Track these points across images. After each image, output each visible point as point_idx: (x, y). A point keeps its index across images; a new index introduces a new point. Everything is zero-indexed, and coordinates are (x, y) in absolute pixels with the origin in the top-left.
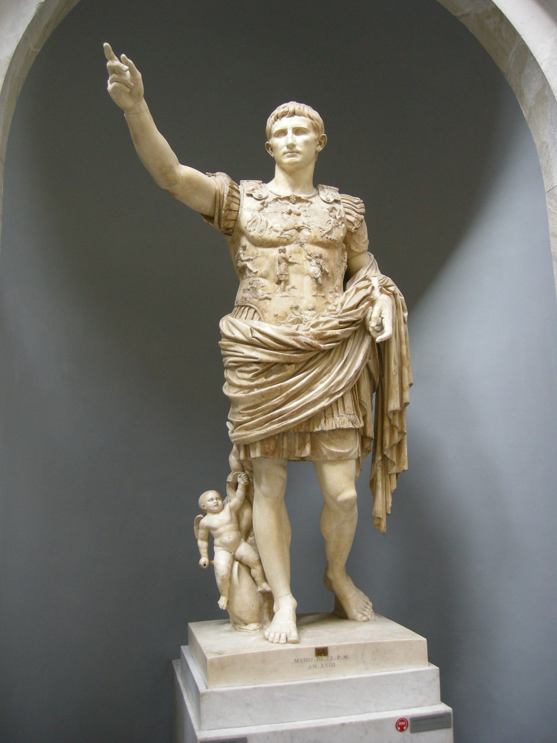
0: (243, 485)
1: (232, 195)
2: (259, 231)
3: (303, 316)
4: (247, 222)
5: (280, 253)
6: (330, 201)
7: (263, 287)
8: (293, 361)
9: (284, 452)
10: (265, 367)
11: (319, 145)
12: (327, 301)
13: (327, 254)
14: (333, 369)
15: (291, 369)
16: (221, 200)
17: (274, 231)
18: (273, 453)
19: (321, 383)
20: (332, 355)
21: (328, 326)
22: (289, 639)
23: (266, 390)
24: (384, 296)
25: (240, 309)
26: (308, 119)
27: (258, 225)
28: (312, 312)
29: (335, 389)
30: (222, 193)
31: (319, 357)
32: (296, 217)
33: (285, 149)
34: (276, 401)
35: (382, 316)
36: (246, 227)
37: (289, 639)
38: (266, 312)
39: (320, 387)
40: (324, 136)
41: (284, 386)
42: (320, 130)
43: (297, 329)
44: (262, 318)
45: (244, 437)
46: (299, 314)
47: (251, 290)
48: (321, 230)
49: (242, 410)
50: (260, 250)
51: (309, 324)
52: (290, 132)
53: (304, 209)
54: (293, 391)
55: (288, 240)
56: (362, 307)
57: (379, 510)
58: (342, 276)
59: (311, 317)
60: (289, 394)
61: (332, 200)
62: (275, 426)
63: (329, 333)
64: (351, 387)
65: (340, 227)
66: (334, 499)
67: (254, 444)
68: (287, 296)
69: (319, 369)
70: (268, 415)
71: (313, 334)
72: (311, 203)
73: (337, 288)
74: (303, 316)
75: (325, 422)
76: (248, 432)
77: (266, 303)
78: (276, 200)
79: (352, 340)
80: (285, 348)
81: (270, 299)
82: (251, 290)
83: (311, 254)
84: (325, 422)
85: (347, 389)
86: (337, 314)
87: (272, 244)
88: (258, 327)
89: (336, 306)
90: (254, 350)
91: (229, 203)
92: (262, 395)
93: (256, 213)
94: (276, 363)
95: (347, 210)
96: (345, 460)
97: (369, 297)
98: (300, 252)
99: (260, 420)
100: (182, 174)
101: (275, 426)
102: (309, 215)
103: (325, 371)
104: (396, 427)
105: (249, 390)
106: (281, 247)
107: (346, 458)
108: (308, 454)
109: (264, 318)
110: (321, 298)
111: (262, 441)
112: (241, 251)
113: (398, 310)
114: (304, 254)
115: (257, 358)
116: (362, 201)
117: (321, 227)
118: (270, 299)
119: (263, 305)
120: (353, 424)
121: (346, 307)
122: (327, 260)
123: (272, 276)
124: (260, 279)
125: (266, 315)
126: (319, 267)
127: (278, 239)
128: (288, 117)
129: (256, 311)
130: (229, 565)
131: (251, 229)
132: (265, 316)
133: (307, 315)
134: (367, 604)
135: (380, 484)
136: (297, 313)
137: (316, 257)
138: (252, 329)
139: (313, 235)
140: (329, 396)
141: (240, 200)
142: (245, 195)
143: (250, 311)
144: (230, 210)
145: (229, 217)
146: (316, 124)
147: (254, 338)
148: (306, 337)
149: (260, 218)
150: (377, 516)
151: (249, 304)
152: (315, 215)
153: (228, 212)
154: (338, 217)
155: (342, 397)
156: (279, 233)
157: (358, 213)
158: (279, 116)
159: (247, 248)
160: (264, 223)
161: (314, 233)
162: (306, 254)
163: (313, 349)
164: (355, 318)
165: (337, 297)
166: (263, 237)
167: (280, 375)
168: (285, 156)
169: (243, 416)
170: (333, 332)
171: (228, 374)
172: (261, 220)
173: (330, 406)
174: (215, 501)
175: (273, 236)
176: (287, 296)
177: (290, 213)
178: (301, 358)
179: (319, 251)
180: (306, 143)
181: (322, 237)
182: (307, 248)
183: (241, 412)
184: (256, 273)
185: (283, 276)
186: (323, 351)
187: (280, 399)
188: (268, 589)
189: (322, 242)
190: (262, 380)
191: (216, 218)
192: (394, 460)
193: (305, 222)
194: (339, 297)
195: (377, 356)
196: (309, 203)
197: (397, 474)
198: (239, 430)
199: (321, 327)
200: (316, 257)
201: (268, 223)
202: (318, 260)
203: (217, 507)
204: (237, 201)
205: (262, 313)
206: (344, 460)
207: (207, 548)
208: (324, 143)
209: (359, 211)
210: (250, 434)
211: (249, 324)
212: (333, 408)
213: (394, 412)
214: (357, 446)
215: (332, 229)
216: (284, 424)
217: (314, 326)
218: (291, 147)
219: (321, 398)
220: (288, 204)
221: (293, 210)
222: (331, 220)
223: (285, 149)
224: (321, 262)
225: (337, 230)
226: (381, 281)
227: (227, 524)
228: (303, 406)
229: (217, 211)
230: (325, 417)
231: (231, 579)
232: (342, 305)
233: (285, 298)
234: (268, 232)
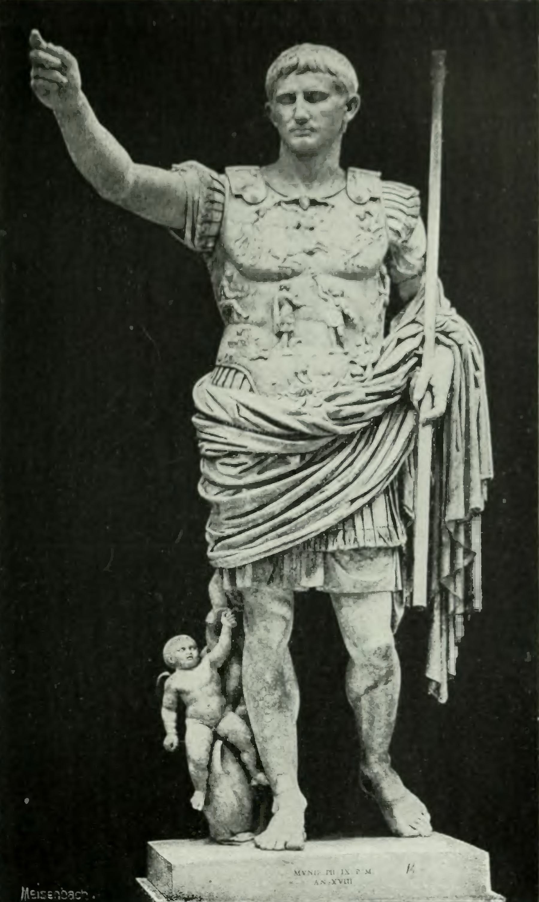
0: (229, 627)
4: (234, 241)
10: (257, 460)
17: (272, 256)
20: (355, 440)
22: (288, 845)
25: (223, 371)
26: (328, 76)
30: (196, 198)
33: (292, 124)
35: (432, 383)
37: (288, 845)
44: (254, 388)
47: (240, 344)
52: (300, 98)
55: (293, 270)
61: (366, 198)
67: (242, 568)
78: (279, 204)
79: (386, 418)
84: (344, 538)
86: (365, 380)
89: (365, 368)
104: (460, 544)
105: (235, 490)
106: (284, 282)
116: (416, 192)
120: (385, 541)
121: (379, 369)
128: (297, 74)
129: (245, 377)
137: (335, 296)
138: (239, 405)
141: (223, 205)
144: (210, 222)
145: (207, 233)
158: (284, 72)
163: (325, 434)
166: (257, 267)
168: (292, 134)
171: (204, 467)
174: (188, 651)
177: (298, 227)
184: (247, 318)
186: (342, 436)
188: (266, 782)
190: (252, 478)
198: (223, 548)
199: (340, 401)
200: (335, 296)
203: (190, 660)
213: (457, 523)
218: (302, 122)
222: (360, 235)
226: (438, 325)
232: (374, 365)
234: (263, 258)
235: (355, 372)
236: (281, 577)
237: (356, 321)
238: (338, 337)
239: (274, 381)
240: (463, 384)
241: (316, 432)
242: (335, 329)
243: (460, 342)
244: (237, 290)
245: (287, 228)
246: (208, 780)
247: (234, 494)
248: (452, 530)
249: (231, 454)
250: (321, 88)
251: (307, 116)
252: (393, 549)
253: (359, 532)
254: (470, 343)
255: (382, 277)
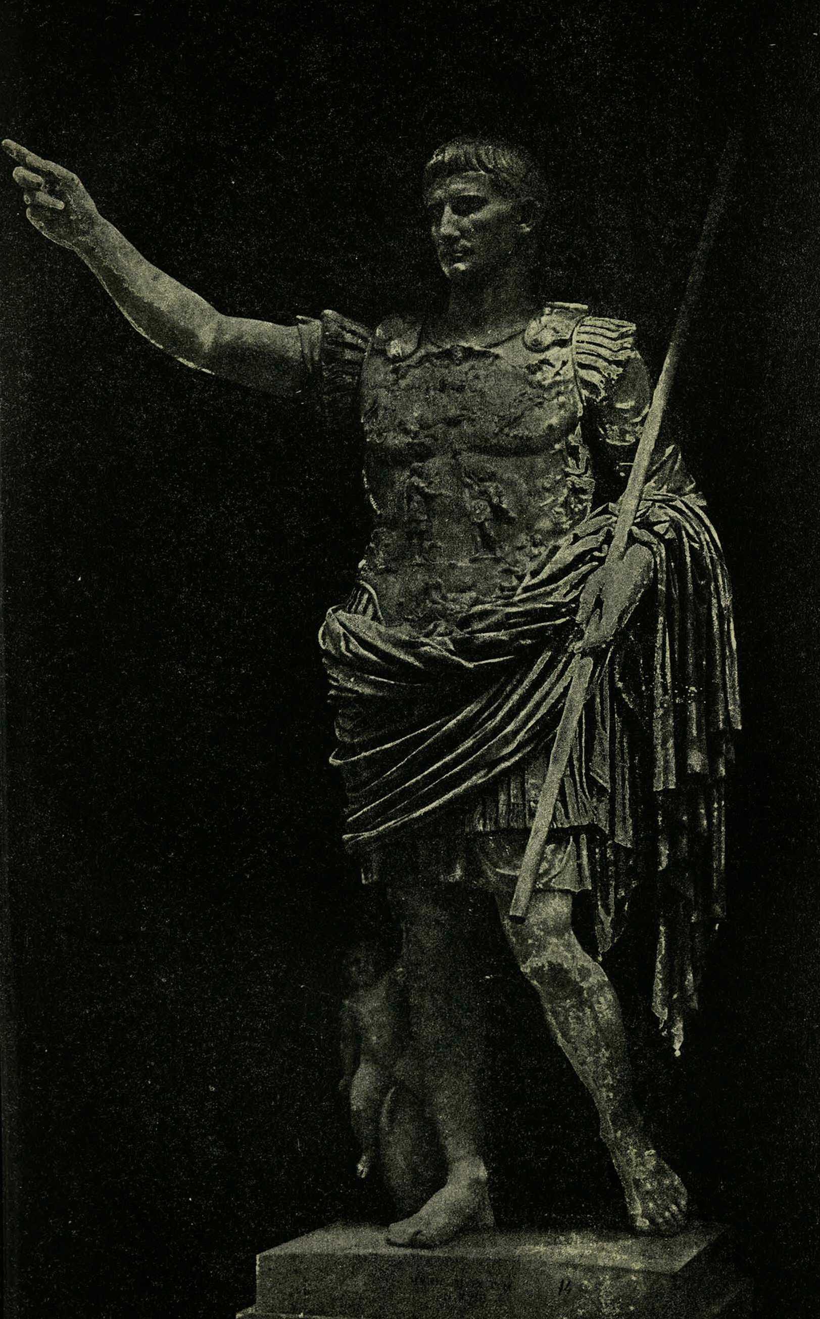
72: (497, 357)
89: (521, 578)
126: (485, 500)
157: (610, 362)
237: (512, 514)
238: (485, 536)
242: (481, 526)
253: (502, 808)
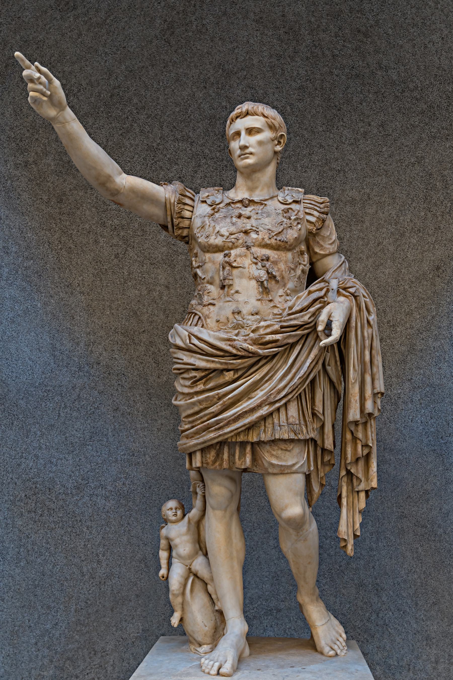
1: (183, 203)
2: (206, 236)
3: (245, 321)
5: (225, 257)
6: (288, 203)
7: (208, 293)
8: (230, 367)
9: (225, 463)
10: (203, 374)
11: (278, 144)
12: (274, 305)
13: (276, 256)
14: (276, 376)
15: (229, 376)
16: (172, 208)
17: (220, 235)
18: (214, 462)
19: (262, 390)
20: (274, 361)
21: (269, 330)
23: (204, 398)
24: (342, 299)
26: (262, 118)
27: (207, 230)
28: (255, 317)
29: (275, 397)
30: (172, 201)
31: (261, 364)
32: (246, 221)
33: (238, 152)
34: (213, 409)
35: (331, 319)
36: (195, 234)
38: (209, 318)
39: (259, 395)
40: (282, 135)
41: (222, 394)
42: (277, 128)
43: (237, 335)
44: (205, 325)
45: (184, 446)
46: (241, 319)
48: (270, 232)
49: (184, 418)
50: (208, 255)
51: (250, 328)
52: (243, 133)
53: (257, 211)
54: (229, 399)
55: (233, 243)
56: (312, 309)
57: (343, 531)
58: (299, 278)
59: (253, 322)
60: (226, 401)
61: (290, 201)
62: (212, 435)
63: (269, 338)
64: (296, 395)
65: (295, 228)
66: (280, 516)
67: (195, 452)
68: (229, 301)
69: (259, 375)
70: (204, 424)
71: (252, 340)
72: (266, 205)
73: (288, 291)
74: (245, 321)
75: (265, 431)
76: (187, 441)
77: (210, 309)
78: (228, 204)
80: (222, 354)
81: (214, 305)
82: (198, 296)
83: (257, 257)
84: (265, 431)
85: (290, 396)
87: (218, 249)
88: (196, 334)
89: (284, 310)
90: (192, 356)
91: (180, 211)
92: (200, 402)
93: (206, 219)
94: (215, 370)
95: (307, 211)
96: (288, 473)
97: (322, 299)
98: (245, 256)
99: (197, 429)
100: (124, 183)
101: (212, 435)
102: (260, 217)
103: (267, 378)
104: (359, 439)
106: (226, 252)
107: (289, 471)
108: (247, 466)
109: (207, 324)
110: (267, 302)
111: (202, 450)
112: (193, 259)
113: (362, 313)
114: (250, 257)
115: (194, 365)
117: (271, 229)
118: (214, 305)
119: (205, 310)
120: (295, 434)
121: (294, 310)
122: (275, 263)
123: (217, 281)
124: (207, 285)
125: (209, 321)
127: (223, 243)
129: (200, 318)
130: (182, 580)
131: (199, 235)
132: (207, 322)
133: (248, 320)
134: (341, 636)
135: (344, 501)
136: (238, 317)
137: (262, 260)
139: (260, 237)
140: (268, 404)
141: (193, 207)
142: (200, 202)
143: (195, 318)
144: (183, 218)
145: (181, 225)
146: (272, 123)
147: (191, 345)
148: (242, 342)
149: (209, 224)
150: (341, 537)
151: (194, 311)
152: (266, 217)
153: (180, 220)
154: (293, 218)
155: (286, 405)
156: (225, 237)
157: (320, 213)
159: (198, 254)
160: (211, 229)
161: (263, 235)
162: (252, 257)
164: (301, 322)
165: (288, 300)
166: (209, 243)
167: (218, 382)
168: (239, 159)
169: (186, 424)
170: (273, 337)
172: (209, 225)
173: (271, 414)
175: (219, 241)
176: (229, 301)
178: (240, 364)
179: (267, 253)
180: (260, 143)
181: (270, 238)
182: (253, 251)
183: (183, 419)
185: (226, 280)
187: (217, 407)
189: (270, 244)
190: (200, 387)
191: (170, 226)
192: (360, 476)
193: (254, 225)
194: (291, 301)
195: (339, 363)
196: (264, 205)
197: (367, 492)
200: (262, 260)
201: (215, 228)
202: (266, 262)
204: (191, 209)
205: (205, 319)
206: (286, 473)
207: (167, 559)
208: (284, 142)
209: (322, 210)
210: (189, 443)
211: (189, 330)
212: (274, 416)
213: (356, 423)
214: (304, 458)
215: (283, 230)
216: (221, 433)
217: (253, 331)
219: (260, 406)
220: (241, 208)
221: (243, 213)
223: (238, 152)
224: (267, 266)
225: (290, 231)
226: (341, 283)
227: (183, 535)
228: (240, 414)
229: (169, 219)
230: (265, 426)
231: (183, 594)
233: (228, 303)
234: (214, 237)
235: (275, 312)
236: (222, 460)
239: (218, 318)
240: (359, 325)
241: (243, 353)
242: (262, 282)
243: (356, 294)
244: (199, 262)
245: (232, 217)
246: (182, 604)
247: (190, 399)
248: (353, 428)
249: (187, 370)
250: (257, 125)
251: (247, 145)
252: (306, 441)
254: (364, 296)
255: (302, 253)
